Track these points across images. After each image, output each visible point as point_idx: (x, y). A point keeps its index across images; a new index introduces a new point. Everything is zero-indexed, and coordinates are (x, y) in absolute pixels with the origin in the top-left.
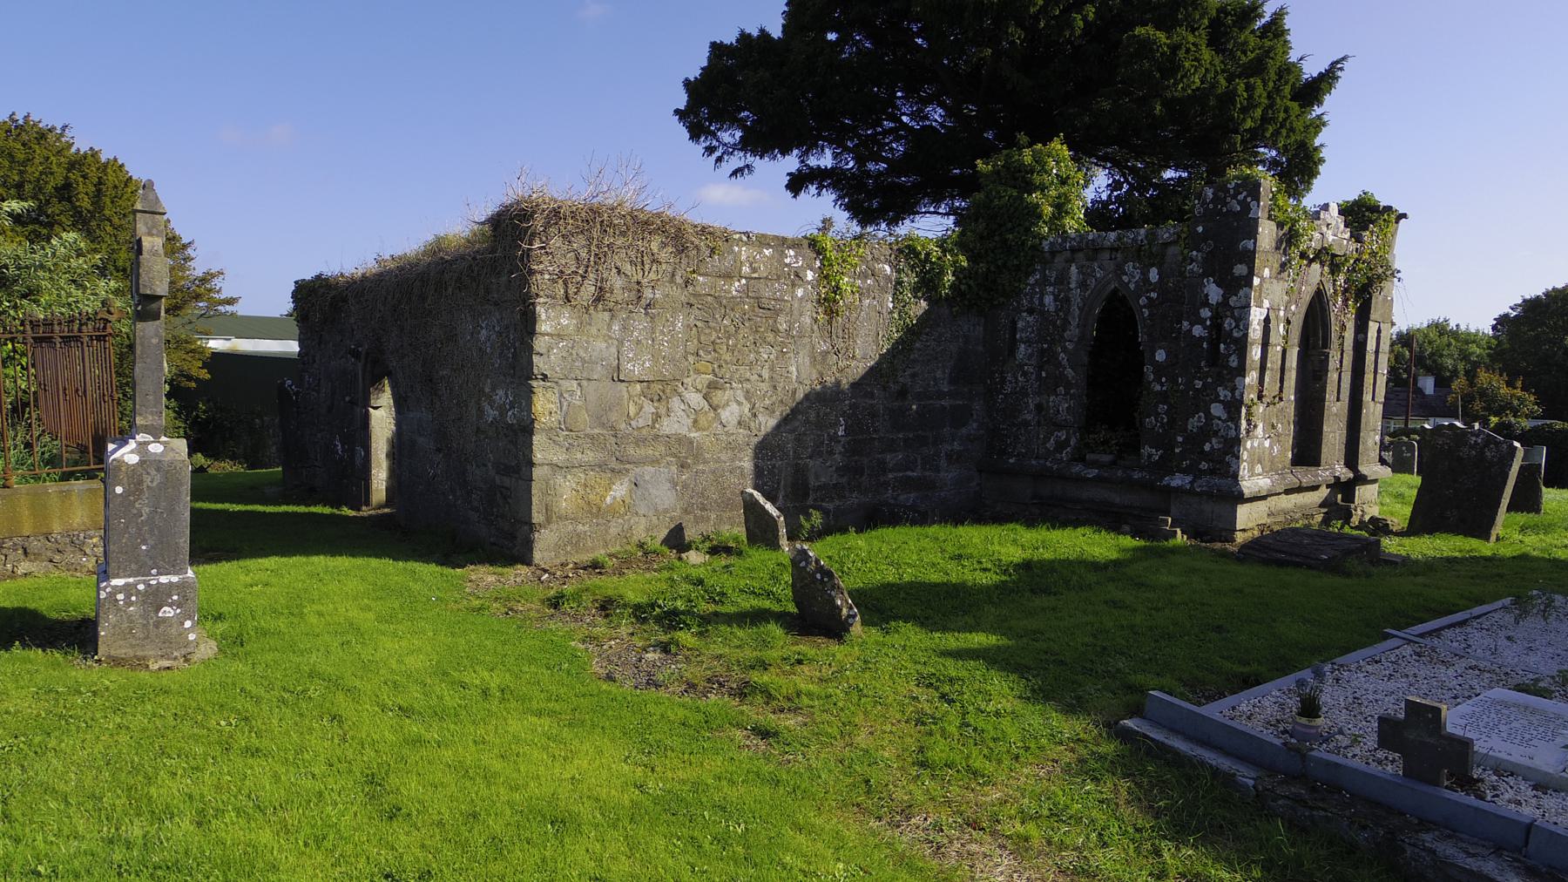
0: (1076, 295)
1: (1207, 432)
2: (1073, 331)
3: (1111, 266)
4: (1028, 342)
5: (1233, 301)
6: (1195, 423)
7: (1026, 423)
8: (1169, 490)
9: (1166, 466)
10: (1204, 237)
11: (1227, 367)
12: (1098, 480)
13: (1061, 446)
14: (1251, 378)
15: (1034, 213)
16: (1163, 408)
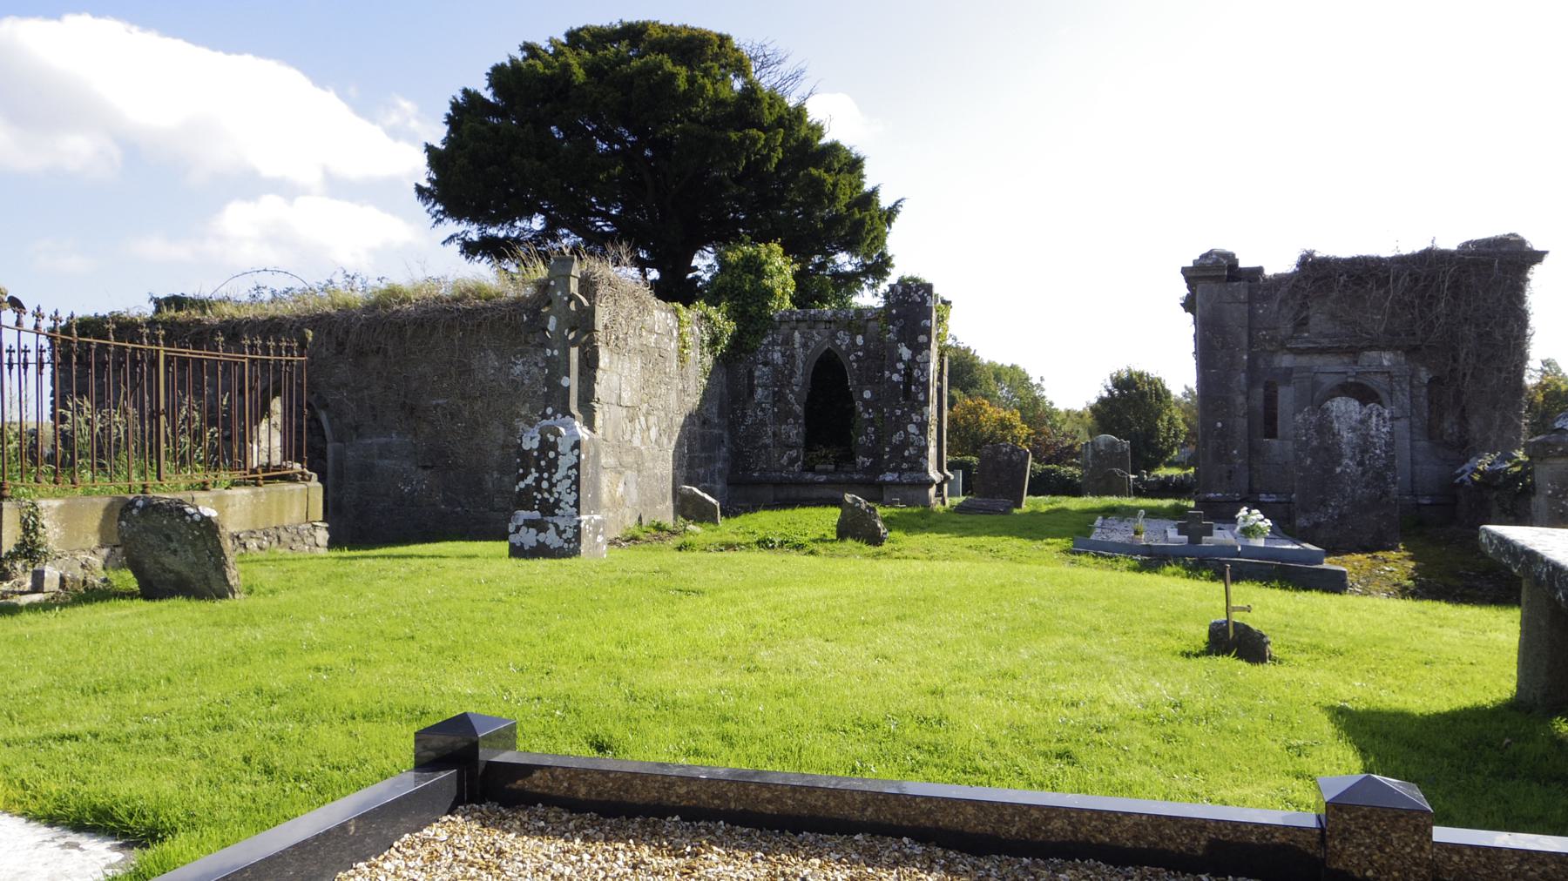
0: (799, 352)
1: (906, 443)
2: (798, 378)
3: (827, 333)
4: (765, 386)
5: (918, 358)
6: (897, 437)
7: (766, 446)
8: (885, 483)
9: (878, 468)
10: (898, 316)
11: (916, 400)
12: (828, 483)
13: (792, 462)
14: (932, 409)
15: (770, 293)
16: (871, 429)
